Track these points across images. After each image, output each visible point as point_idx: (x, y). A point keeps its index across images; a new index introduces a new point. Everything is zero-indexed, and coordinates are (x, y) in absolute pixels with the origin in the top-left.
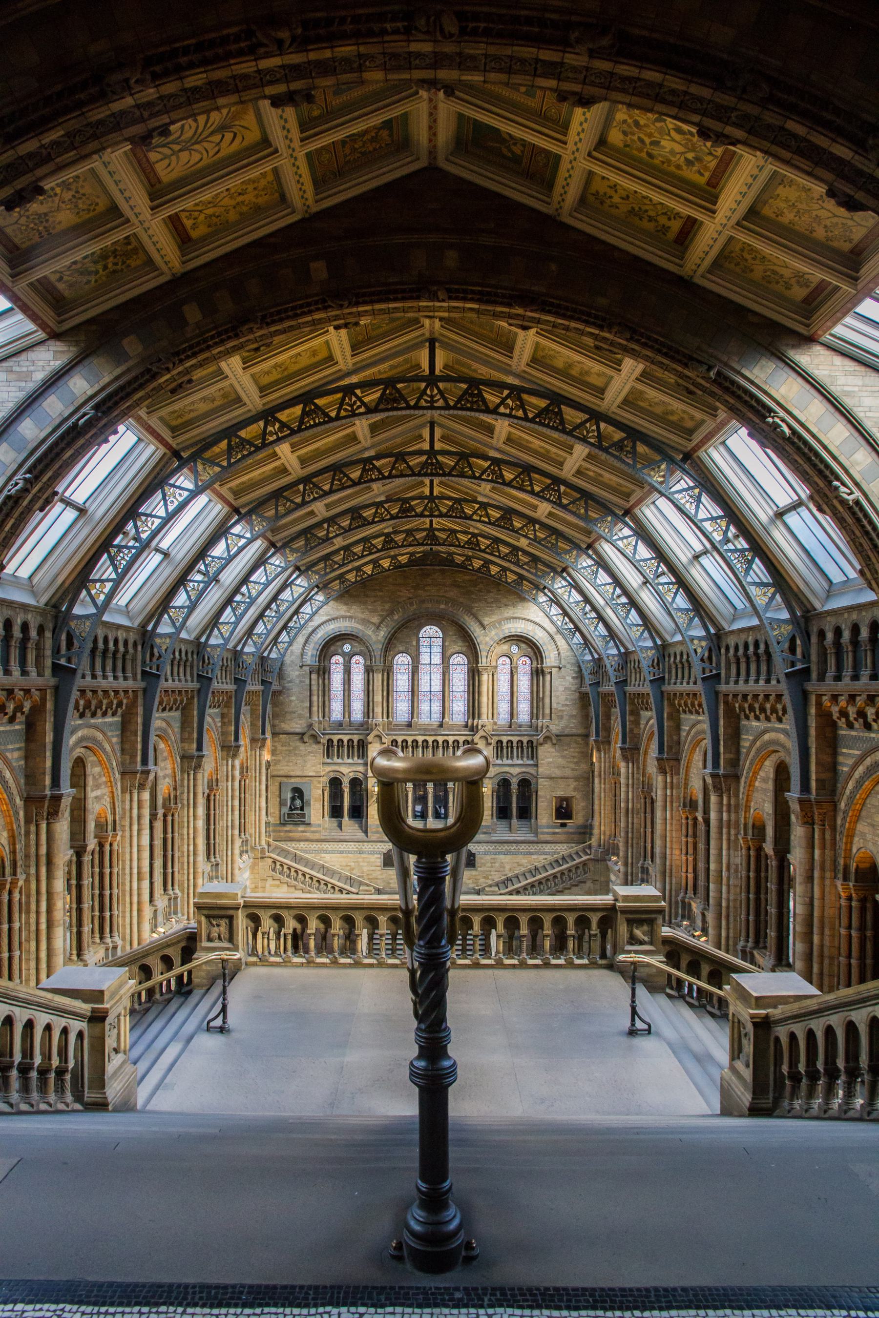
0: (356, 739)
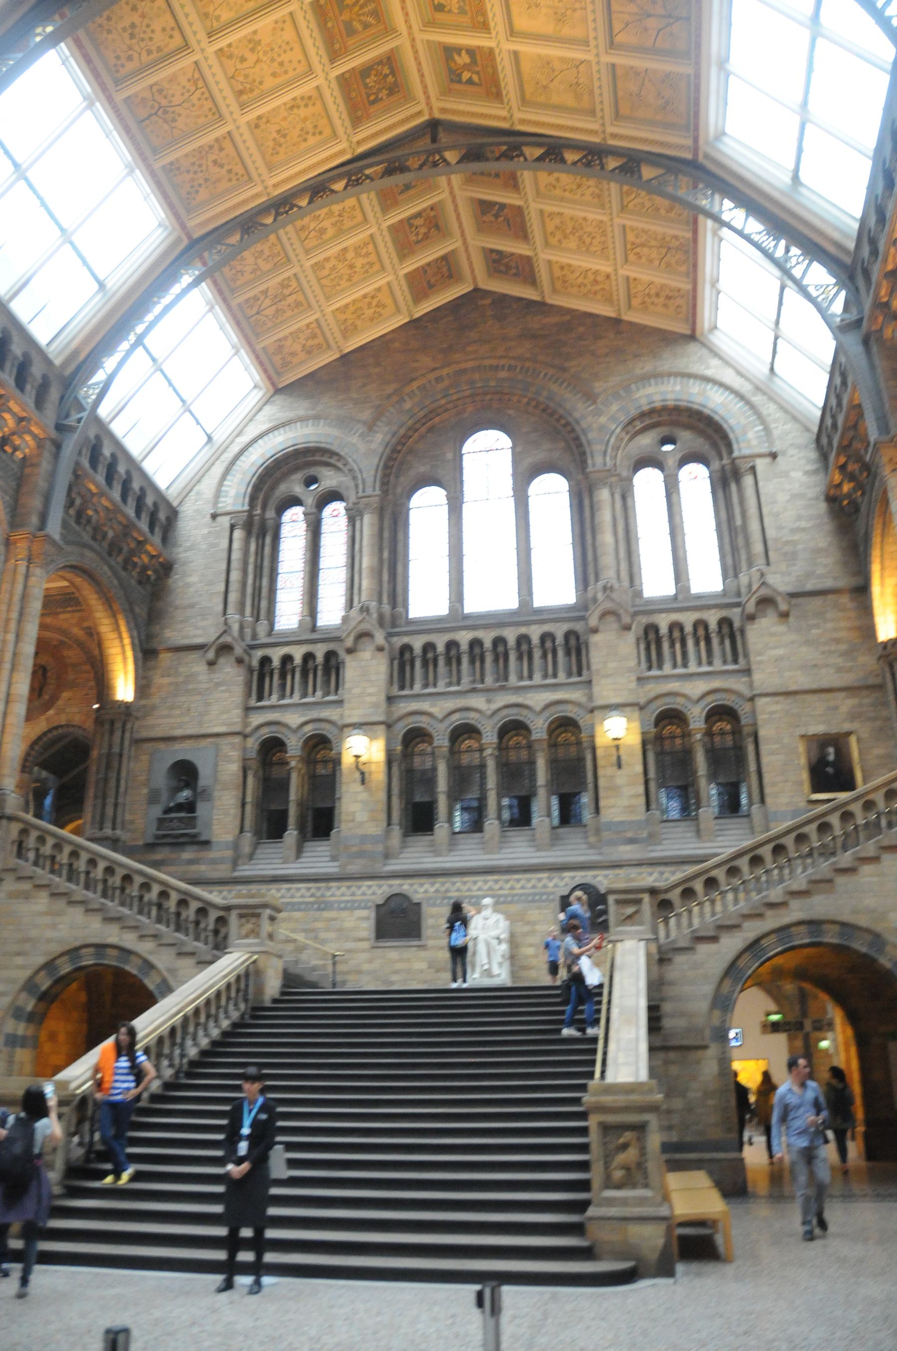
0: (320, 651)
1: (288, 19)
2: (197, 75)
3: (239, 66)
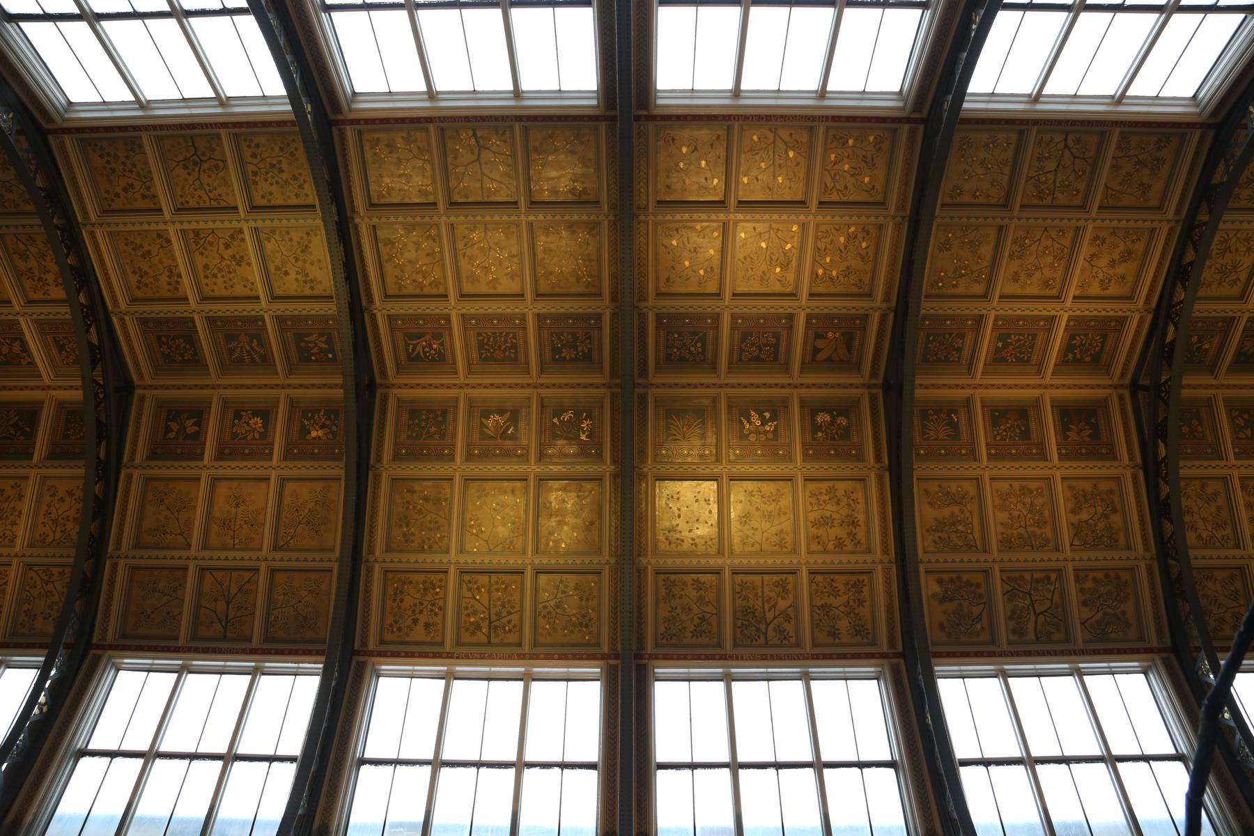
1: (253, 293)
2: (223, 204)
3: (222, 241)
